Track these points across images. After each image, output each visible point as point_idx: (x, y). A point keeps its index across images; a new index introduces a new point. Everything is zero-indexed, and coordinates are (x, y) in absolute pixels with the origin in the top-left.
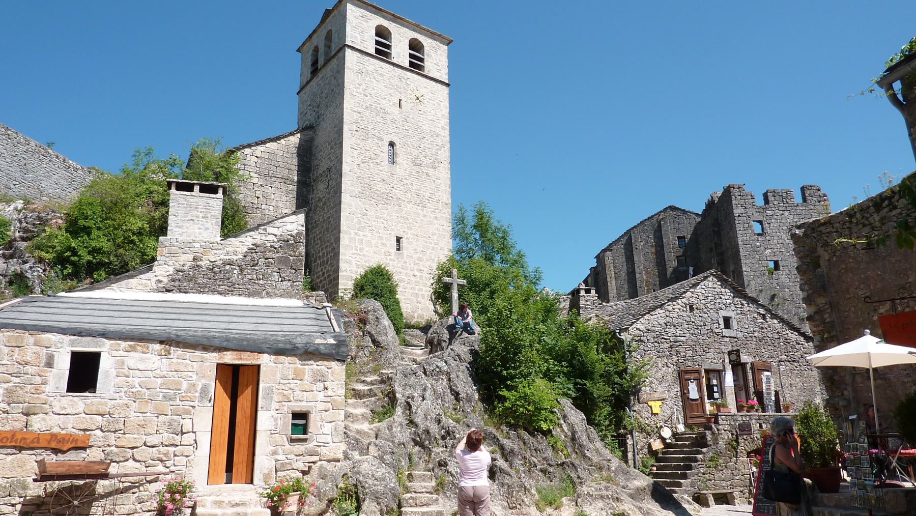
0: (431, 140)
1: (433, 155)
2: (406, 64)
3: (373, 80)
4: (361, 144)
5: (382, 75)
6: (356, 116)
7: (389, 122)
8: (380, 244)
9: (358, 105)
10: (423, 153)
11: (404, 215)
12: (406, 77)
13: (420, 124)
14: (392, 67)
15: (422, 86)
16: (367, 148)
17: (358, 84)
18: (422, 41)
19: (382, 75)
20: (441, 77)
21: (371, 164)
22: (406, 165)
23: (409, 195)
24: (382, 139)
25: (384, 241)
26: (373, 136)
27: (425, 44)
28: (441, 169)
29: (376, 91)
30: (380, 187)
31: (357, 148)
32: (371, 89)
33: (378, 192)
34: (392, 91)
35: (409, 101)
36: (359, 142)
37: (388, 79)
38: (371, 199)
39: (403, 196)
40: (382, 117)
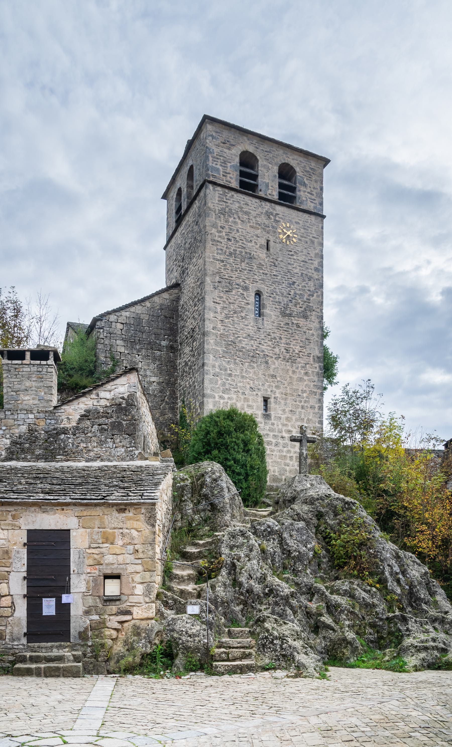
0: (303, 285)
1: (305, 302)
2: (276, 197)
3: (237, 220)
4: (225, 297)
5: (247, 213)
6: (218, 265)
7: (255, 267)
8: (246, 406)
9: (220, 252)
10: (294, 301)
11: (272, 373)
12: (275, 212)
13: (290, 267)
14: (257, 201)
15: (294, 221)
16: (231, 301)
17: (221, 227)
18: (294, 165)
19: (247, 213)
20: (315, 208)
21: (236, 319)
22: (273, 316)
23: (277, 350)
24: (246, 289)
25: (250, 403)
26: (237, 286)
27: (297, 169)
28: (313, 318)
29: (240, 234)
30: (245, 344)
31: (220, 302)
32: (235, 231)
33: (244, 350)
34: (259, 231)
35: (278, 240)
36: (222, 295)
37: (255, 217)
38: (236, 358)
39: (271, 352)
40: (247, 263)
